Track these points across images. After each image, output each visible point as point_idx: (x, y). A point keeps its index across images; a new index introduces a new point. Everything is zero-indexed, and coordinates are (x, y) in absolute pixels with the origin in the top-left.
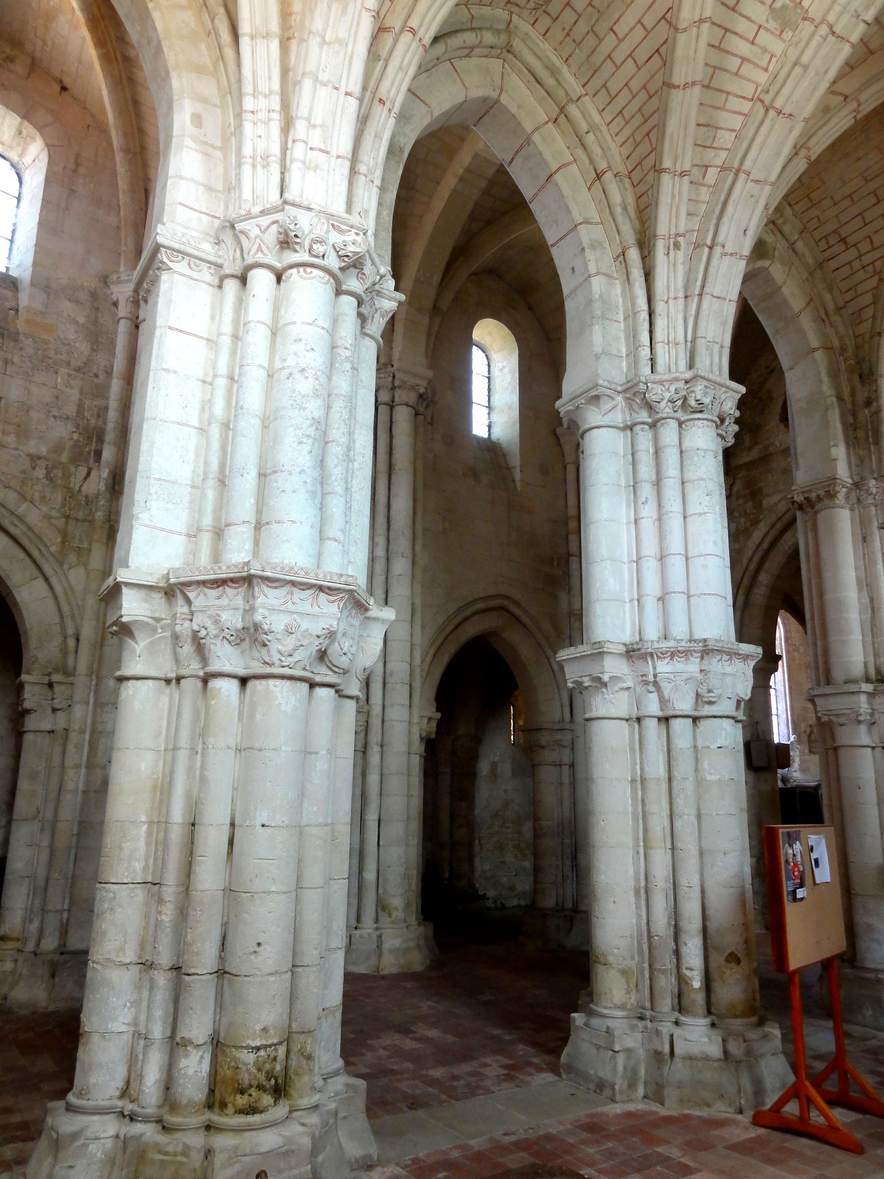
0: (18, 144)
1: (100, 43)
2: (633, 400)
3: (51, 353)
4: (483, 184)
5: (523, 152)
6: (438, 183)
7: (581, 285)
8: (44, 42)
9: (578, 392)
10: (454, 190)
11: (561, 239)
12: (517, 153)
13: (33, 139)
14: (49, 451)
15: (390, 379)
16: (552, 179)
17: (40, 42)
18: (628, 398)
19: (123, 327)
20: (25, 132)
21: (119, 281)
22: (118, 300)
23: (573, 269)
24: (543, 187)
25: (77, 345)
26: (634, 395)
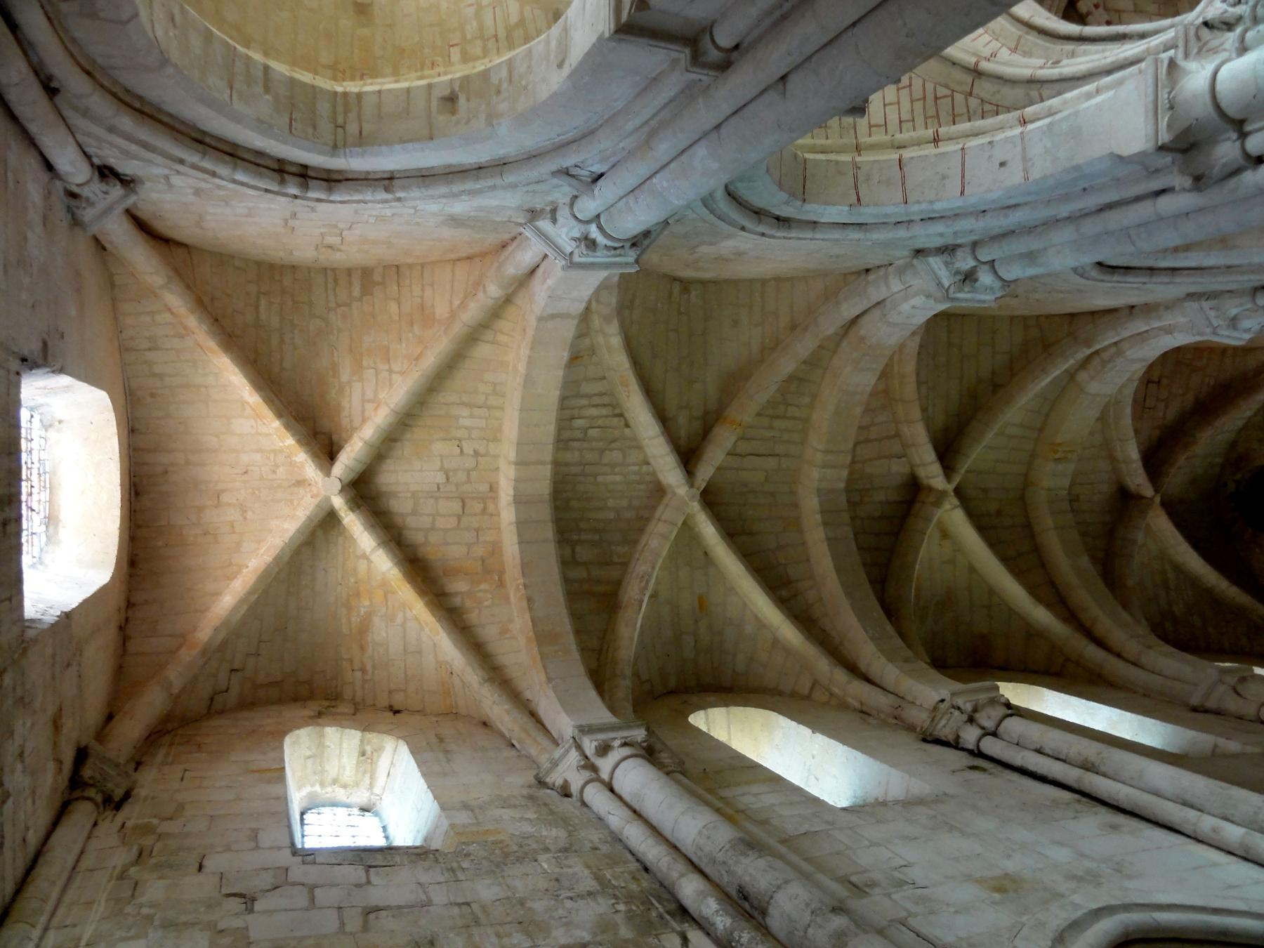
0: (365, 772)
1: (422, 592)
2: (1205, 44)
3: (515, 848)
4: (846, 517)
5: (861, 178)
6: (808, 560)
7: (1024, 149)
8: (363, 670)
9: (1151, 98)
10: (828, 539)
11: (963, 177)
12: (856, 187)
13: (379, 749)
14: (595, 935)
15: (957, 713)
16: (903, 162)
17: (358, 674)
18: (1199, 52)
19: (597, 798)
20: (368, 748)
21: (555, 764)
22: (566, 781)
23: (1002, 164)
24: (903, 177)
25: (544, 833)
26: (1198, 38)
